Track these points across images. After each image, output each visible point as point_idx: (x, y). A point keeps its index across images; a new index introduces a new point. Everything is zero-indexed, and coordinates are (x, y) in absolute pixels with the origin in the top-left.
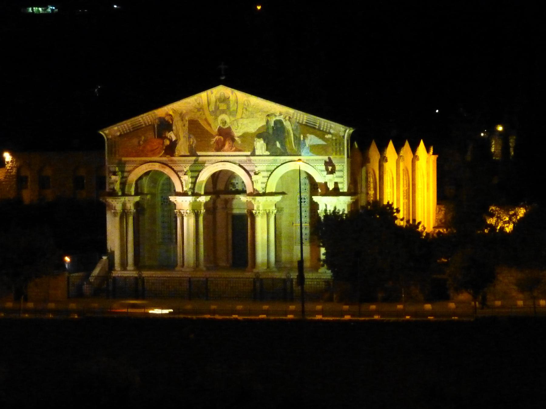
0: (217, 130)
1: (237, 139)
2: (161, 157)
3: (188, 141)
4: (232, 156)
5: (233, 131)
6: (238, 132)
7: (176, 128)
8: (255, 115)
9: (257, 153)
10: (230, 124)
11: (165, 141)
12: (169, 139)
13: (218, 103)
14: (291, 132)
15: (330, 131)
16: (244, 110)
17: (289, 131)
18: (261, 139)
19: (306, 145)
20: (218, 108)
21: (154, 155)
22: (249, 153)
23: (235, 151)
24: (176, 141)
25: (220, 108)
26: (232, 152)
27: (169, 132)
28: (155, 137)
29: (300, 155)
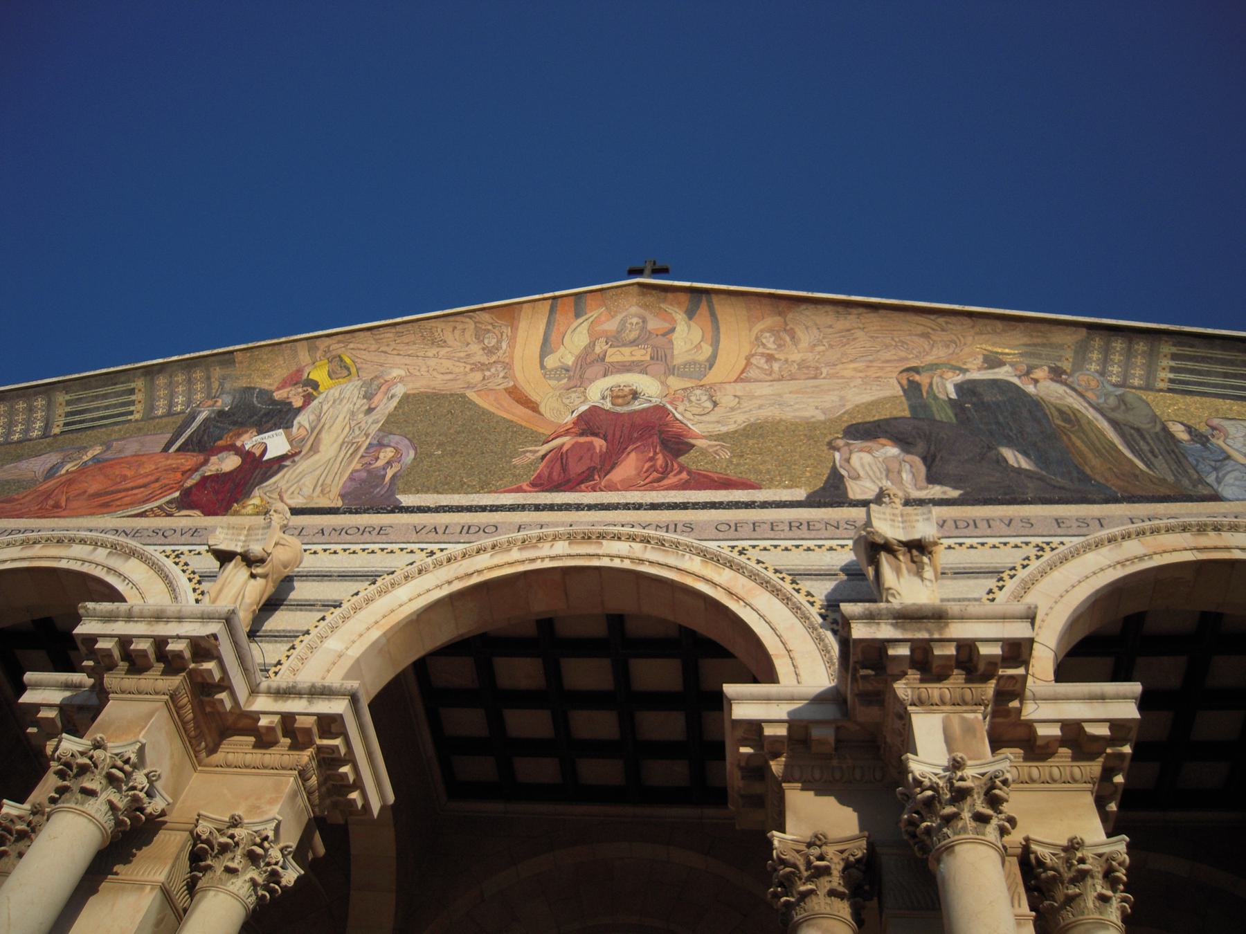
0: (569, 419)
4: (654, 507)
5: (677, 419)
6: (718, 422)
7: (319, 419)
8: (825, 371)
10: (668, 399)
12: (247, 456)
14: (1091, 414)
17: (1075, 412)
18: (883, 441)
19: (1228, 457)
20: (603, 359)
23: (684, 486)
24: (284, 458)
26: (673, 493)
27: (260, 433)
29: (1216, 498)
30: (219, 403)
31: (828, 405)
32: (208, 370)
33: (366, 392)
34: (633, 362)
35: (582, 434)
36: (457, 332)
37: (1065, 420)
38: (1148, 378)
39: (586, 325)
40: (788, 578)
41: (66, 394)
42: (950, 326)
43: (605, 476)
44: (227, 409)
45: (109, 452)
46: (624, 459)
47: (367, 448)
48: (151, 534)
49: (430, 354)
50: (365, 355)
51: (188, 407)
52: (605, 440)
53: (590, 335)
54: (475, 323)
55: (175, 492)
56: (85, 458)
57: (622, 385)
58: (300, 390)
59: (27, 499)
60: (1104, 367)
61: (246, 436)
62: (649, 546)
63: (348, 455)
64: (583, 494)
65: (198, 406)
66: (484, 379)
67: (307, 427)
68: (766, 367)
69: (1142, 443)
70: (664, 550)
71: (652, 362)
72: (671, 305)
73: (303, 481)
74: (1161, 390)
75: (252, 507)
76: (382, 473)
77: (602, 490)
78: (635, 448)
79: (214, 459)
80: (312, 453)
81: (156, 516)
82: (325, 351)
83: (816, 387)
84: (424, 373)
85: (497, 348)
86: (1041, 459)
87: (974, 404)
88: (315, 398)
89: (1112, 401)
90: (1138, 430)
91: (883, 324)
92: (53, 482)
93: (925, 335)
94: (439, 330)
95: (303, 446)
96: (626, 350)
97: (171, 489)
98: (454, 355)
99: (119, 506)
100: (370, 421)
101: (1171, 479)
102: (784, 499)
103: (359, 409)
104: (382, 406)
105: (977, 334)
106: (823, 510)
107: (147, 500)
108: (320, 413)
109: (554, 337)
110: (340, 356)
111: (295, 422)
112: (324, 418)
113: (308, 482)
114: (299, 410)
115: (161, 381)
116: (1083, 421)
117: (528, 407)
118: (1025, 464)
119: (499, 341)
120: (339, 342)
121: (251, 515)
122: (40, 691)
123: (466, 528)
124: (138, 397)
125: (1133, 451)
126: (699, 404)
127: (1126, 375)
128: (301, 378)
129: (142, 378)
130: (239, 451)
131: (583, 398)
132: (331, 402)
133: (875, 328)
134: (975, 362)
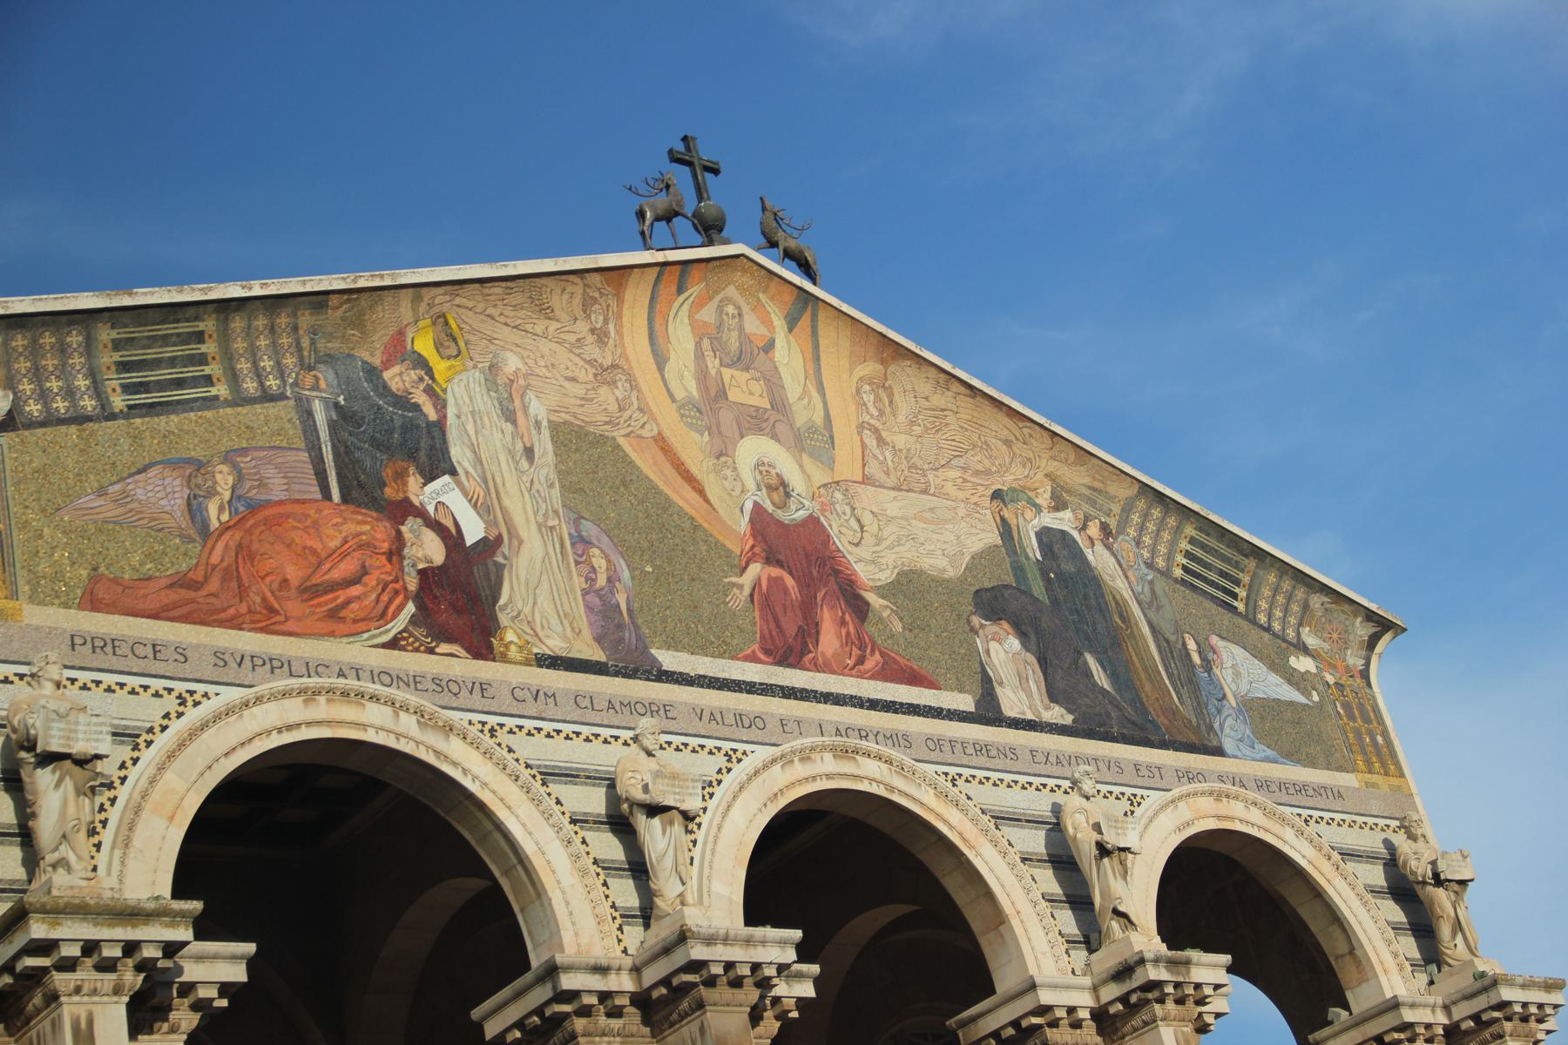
0: (743, 524)
1: (871, 598)
2: (393, 644)
3: (577, 563)
4: (874, 705)
5: (839, 551)
8: (931, 477)
9: (1012, 702)
11: (404, 529)
13: (713, 364)
15: (1299, 634)
16: (871, 442)
18: (1005, 625)
19: (1224, 697)
20: (725, 393)
21: (336, 622)
22: (966, 703)
24: (489, 546)
25: (734, 395)
26: (880, 685)
27: (430, 477)
28: (327, 496)
29: (1219, 752)
30: (323, 385)
31: (950, 550)
32: (295, 315)
33: (500, 403)
34: (758, 409)
35: (768, 561)
36: (566, 297)
37: (1121, 616)
38: (1168, 559)
39: (686, 307)
40: (993, 821)
41: (113, 327)
42: (1032, 440)
43: (817, 644)
44: (341, 399)
45: (248, 484)
46: (822, 617)
47: (573, 545)
48: (434, 686)
49: (539, 330)
50: (468, 316)
51: (284, 382)
52: (793, 578)
53: (693, 329)
54: (585, 285)
55: (406, 599)
56: (227, 495)
57: (766, 460)
58: (414, 374)
59: (214, 584)
60: (1140, 536)
61: (414, 481)
62: (893, 768)
63: (559, 555)
64: (811, 674)
65: (295, 384)
66: (621, 409)
67: (475, 475)
68: (881, 458)
69: (1173, 665)
70: (905, 777)
71: (774, 416)
72: (772, 299)
73: (539, 602)
74: (1176, 580)
75: (513, 648)
76: (614, 601)
77: (824, 672)
78: (823, 601)
79: (404, 529)
80: (515, 543)
81: (417, 650)
82: (429, 304)
83: (932, 510)
84: (549, 375)
85: (607, 334)
86: (1114, 677)
87: (1055, 574)
88: (445, 401)
89: (1147, 589)
90: (1167, 641)
91: (976, 414)
92: (220, 546)
93: (1008, 443)
94: (549, 290)
95: (495, 517)
96: (742, 376)
97: (396, 593)
98: (562, 336)
99: (355, 621)
100: (543, 480)
101: (1194, 720)
102: (962, 708)
103: (513, 444)
104: (535, 439)
105: (1051, 458)
106: (990, 728)
107: (383, 615)
108: (473, 444)
109: (658, 324)
110: (444, 316)
111: (454, 460)
112: (483, 456)
113: (544, 602)
114: (441, 425)
115: (237, 323)
116: (1132, 621)
117: (694, 488)
118: (1107, 686)
119: (606, 321)
120: (445, 294)
121: (520, 663)
122: (572, 975)
123: (738, 717)
124: (209, 348)
125: (1170, 676)
126: (847, 521)
127: (1153, 552)
128: (405, 348)
129: (214, 316)
130: (420, 513)
131: (739, 484)
132: (471, 420)
133: (967, 417)
134: (1045, 496)
